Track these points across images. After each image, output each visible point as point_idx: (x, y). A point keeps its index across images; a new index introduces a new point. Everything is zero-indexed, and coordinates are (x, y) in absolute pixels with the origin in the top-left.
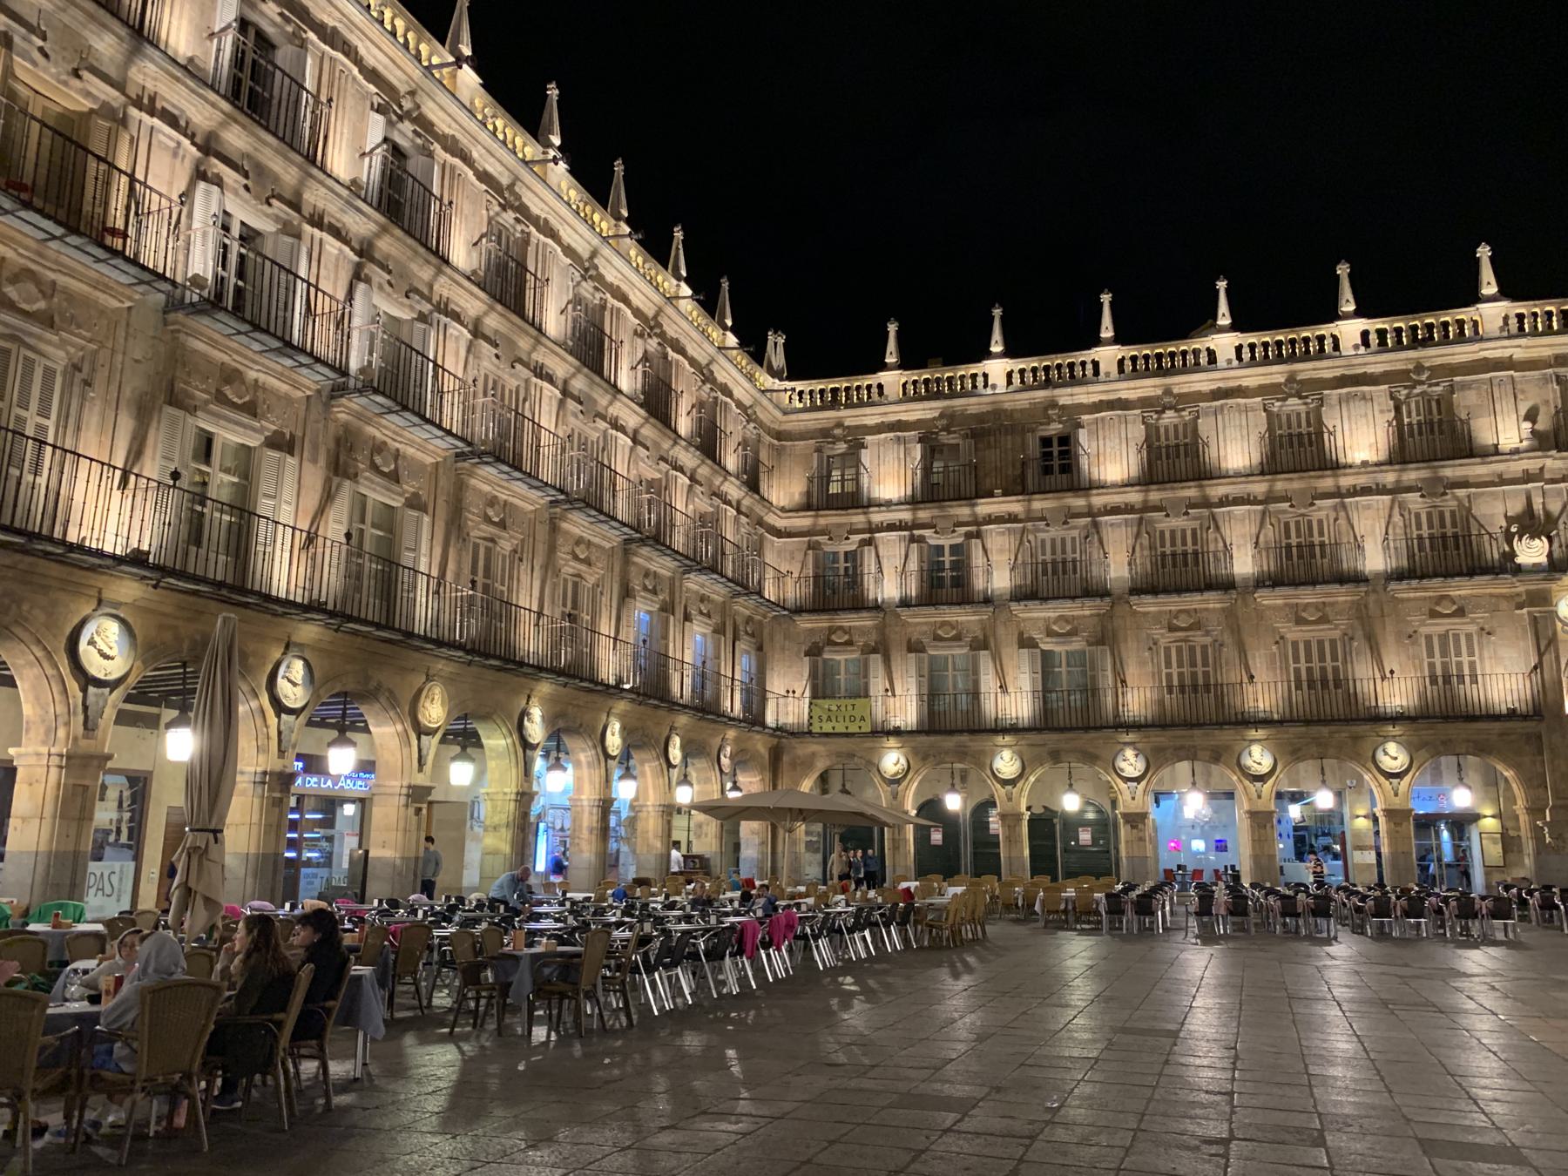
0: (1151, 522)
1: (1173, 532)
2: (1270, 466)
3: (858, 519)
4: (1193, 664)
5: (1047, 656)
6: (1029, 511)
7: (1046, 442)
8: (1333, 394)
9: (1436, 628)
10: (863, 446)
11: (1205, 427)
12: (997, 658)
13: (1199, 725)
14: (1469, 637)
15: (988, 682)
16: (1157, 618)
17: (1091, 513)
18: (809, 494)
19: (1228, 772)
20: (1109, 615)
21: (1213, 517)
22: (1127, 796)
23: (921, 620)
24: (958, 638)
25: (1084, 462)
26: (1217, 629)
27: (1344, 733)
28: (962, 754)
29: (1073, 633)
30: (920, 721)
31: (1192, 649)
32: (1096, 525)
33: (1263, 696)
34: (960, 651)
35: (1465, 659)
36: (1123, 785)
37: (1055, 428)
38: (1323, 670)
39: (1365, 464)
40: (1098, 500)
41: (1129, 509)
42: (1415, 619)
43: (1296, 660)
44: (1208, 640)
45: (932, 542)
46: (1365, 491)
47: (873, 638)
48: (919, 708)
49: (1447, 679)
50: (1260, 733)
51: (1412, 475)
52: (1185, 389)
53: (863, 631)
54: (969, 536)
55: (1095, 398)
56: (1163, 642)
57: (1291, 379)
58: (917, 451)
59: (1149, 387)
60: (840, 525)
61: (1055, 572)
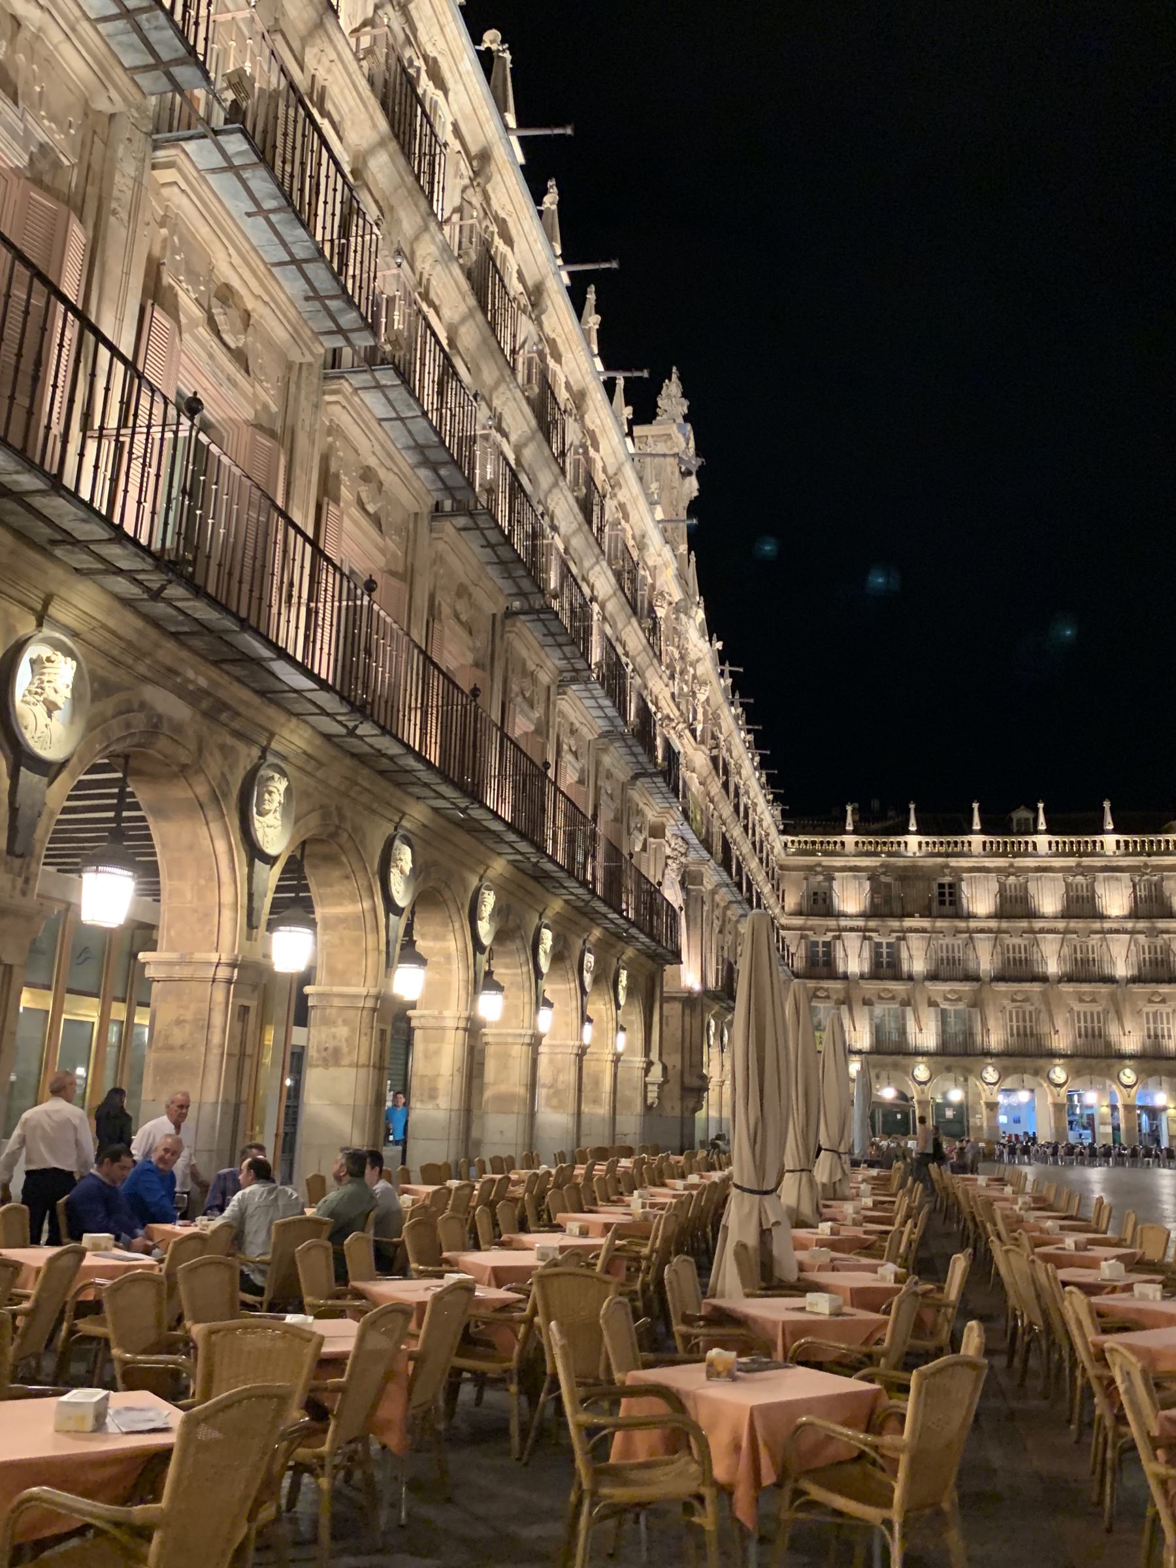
0: (1002, 939)
1: (1014, 946)
2: (1066, 915)
3: (832, 923)
4: (1024, 1021)
5: (944, 1012)
6: (933, 927)
7: (941, 886)
8: (1101, 875)
9: (1150, 1008)
10: (833, 879)
11: (1032, 887)
12: (915, 1011)
13: (1030, 1056)
14: (1168, 1014)
15: (911, 1026)
16: (1005, 994)
17: (968, 931)
18: (800, 904)
19: (1042, 1082)
20: (979, 991)
21: (1036, 938)
22: (988, 1093)
23: (871, 988)
24: (893, 998)
25: (964, 901)
26: (1038, 1003)
27: (1103, 1063)
28: (896, 1066)
29: (959, 999)
30: (871, 1045)
31: (1024, 1013)
32: (971, 938)
33: (1062, 1040)
34: (895, 1006)
35: (1165, 1026)
36: (986, 1087)
37: (947, 880)
38: (1093, 1028)
39: (1117, 917)
40: (973, 924)
41: (990, 931)
42: (1140, 1003)
43: (1079, 1022)
44: (1032, 1008)
45: (876, 940)
46: (1117, 931)
47: (841, 996)
48: (871, 1038)
49: (1156, 1036)
50: (1061, 1061)
51: (1142, 925)
52: (1021, 865)
53: (836, 991)
54: (899, 939)
55: (971, 865)
56: (1008, 1008)
57: (1079, 865)
58: (867, 885)
59: (1001, 862)
60: (820, 926)
61: (948, 964)
